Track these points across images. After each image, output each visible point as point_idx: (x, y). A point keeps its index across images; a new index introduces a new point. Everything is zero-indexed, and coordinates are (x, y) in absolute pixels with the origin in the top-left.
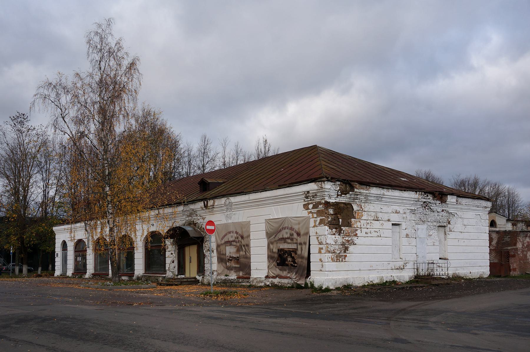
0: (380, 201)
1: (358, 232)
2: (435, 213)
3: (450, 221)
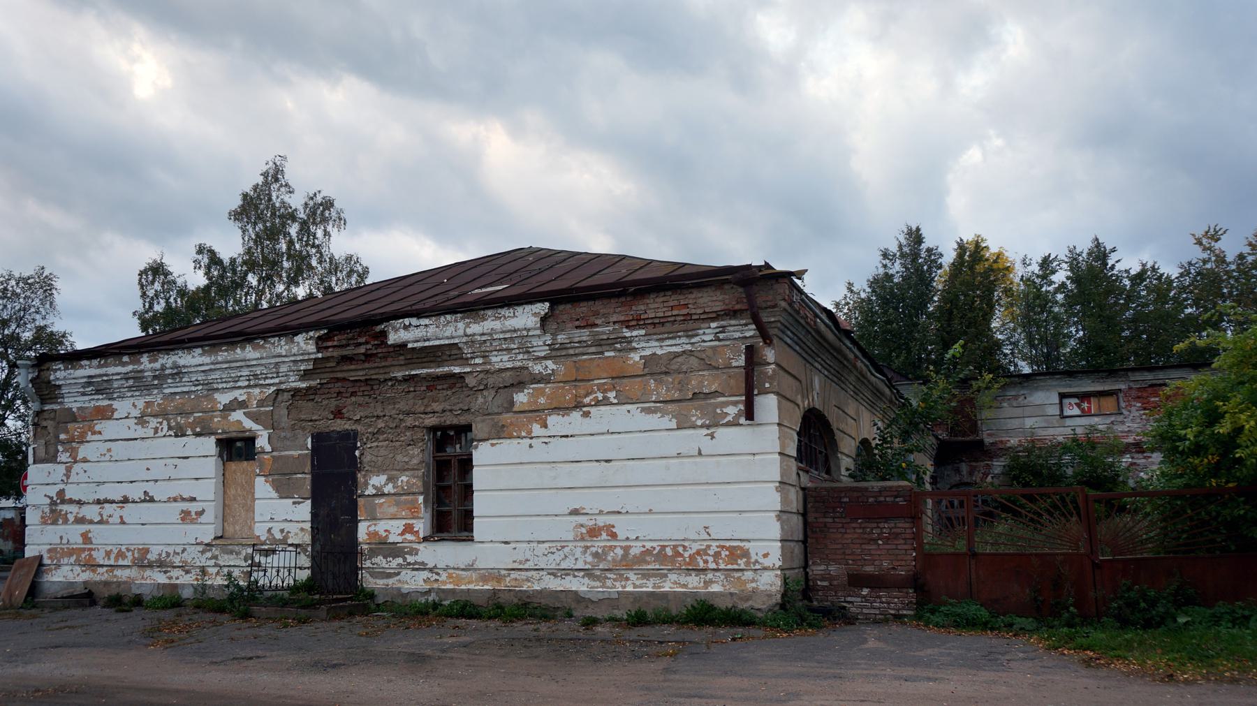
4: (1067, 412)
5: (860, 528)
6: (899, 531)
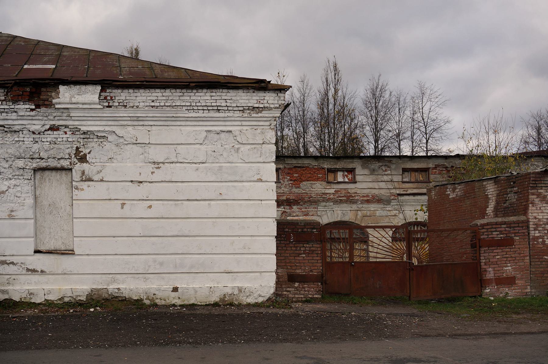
2: (21, 135)
3: (85, 155)
5: (294, 247)
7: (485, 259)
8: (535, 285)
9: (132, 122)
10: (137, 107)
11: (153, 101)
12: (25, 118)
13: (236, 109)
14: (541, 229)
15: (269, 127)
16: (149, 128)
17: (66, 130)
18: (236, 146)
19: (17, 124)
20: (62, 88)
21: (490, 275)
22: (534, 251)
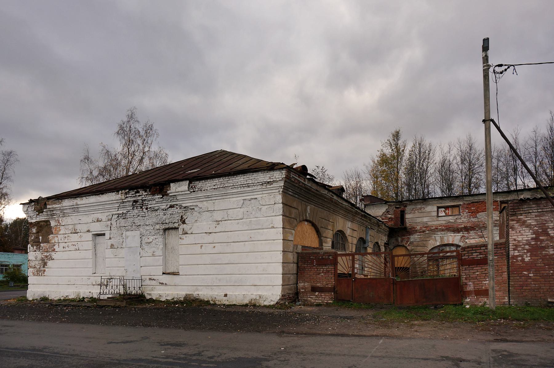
0: (77, 212)
1: (56, 247)
2: (159, 212)
4: (440, 215)
6: (329, 269)
7: (466, 275)
8: (513, 296)
9: (206, 199)
10: (207, 190)
11: (214, 186)
12: (159, 202)
13: (258, 184)
14: (520, 249)
15: (279, 193)
16: (214, 201)
17: (177, 207)
18: (260, 207)
19: (156, 206)
20: (172, 185)
21: (470, 288)
22: (513, 268)
